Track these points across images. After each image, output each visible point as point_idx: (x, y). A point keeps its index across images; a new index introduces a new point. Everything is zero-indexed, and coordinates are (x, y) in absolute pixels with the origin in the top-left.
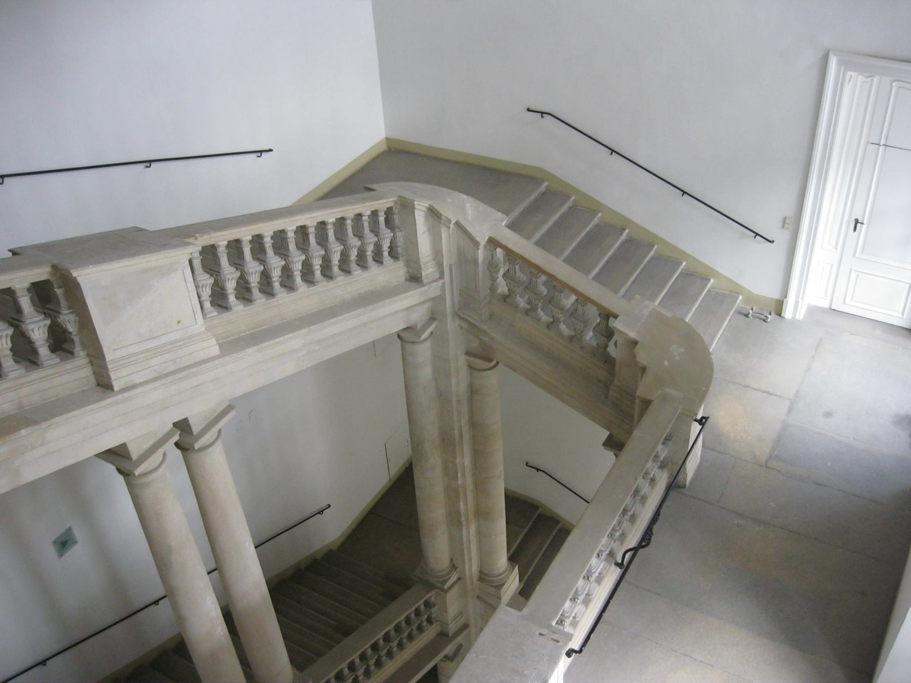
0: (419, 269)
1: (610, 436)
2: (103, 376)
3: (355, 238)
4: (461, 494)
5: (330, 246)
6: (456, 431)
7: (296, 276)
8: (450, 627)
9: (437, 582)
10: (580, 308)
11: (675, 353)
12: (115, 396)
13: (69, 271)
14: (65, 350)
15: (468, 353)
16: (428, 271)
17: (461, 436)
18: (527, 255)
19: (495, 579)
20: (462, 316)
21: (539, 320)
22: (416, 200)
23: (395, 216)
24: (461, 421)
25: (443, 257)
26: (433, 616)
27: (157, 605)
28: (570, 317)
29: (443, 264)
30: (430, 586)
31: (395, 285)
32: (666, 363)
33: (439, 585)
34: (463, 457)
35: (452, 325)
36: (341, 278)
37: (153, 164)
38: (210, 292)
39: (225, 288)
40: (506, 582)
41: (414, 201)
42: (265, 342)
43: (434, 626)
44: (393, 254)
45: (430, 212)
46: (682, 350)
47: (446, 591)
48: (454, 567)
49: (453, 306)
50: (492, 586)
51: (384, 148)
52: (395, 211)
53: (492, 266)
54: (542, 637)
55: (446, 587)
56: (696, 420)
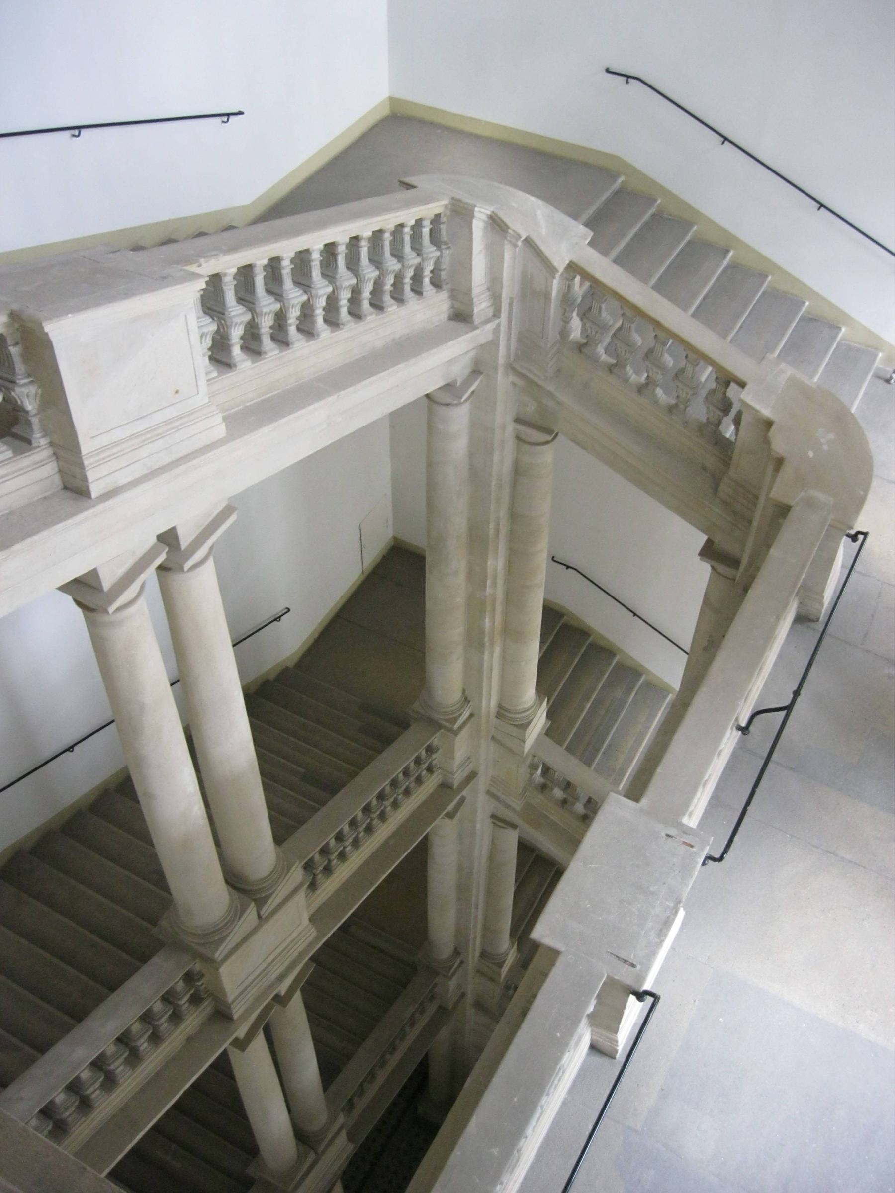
0: (470, 304)
1: (709, 543)
2: (74, 477)
3: (393, 259)
4: (488, 608)
5: (363, 271)
6: (492, 525)
7: (317, 315)
8: (455, 777)
9: (443, 720)
10: (689, 369)
11: (823, 441)
12: (94, 506)
13: (41, 324)
14: (16, 436)
15: (518, 420)
16: (481, 306)
17: (497, 532)
18: (622, 291)
19: (520, 716)
20: (520, 370)
21: (626, 381)
22: (477, 205)
23: (442, 226)
24: (499, 512)
26: (434, 762)
27: (72, 751)
28: (674, 380)
29: (500, 296)
30: (434, 725)
31: (436, 326)
32: (811, 454)
33: (447, 725)
34: (496, 559)
35: (503, 382)
36: (372, 318)
37: (83, 131)
38: (211, 343)
39: (229, 337)
40: (533, 719)
41: (475, 206)
42: (284, 416)
43: (435, 775)
44: (436, 284)
45: (491, 221)
46: (831, 436)
47: (456, 733)
48: (467, 701)
49: (508, 356)
50: (515, 725)
51: (385, 112)
52: (444, 219)
53: (566, 299)
54: (670, 839)
55: (456, 726)
56: (848, 536)
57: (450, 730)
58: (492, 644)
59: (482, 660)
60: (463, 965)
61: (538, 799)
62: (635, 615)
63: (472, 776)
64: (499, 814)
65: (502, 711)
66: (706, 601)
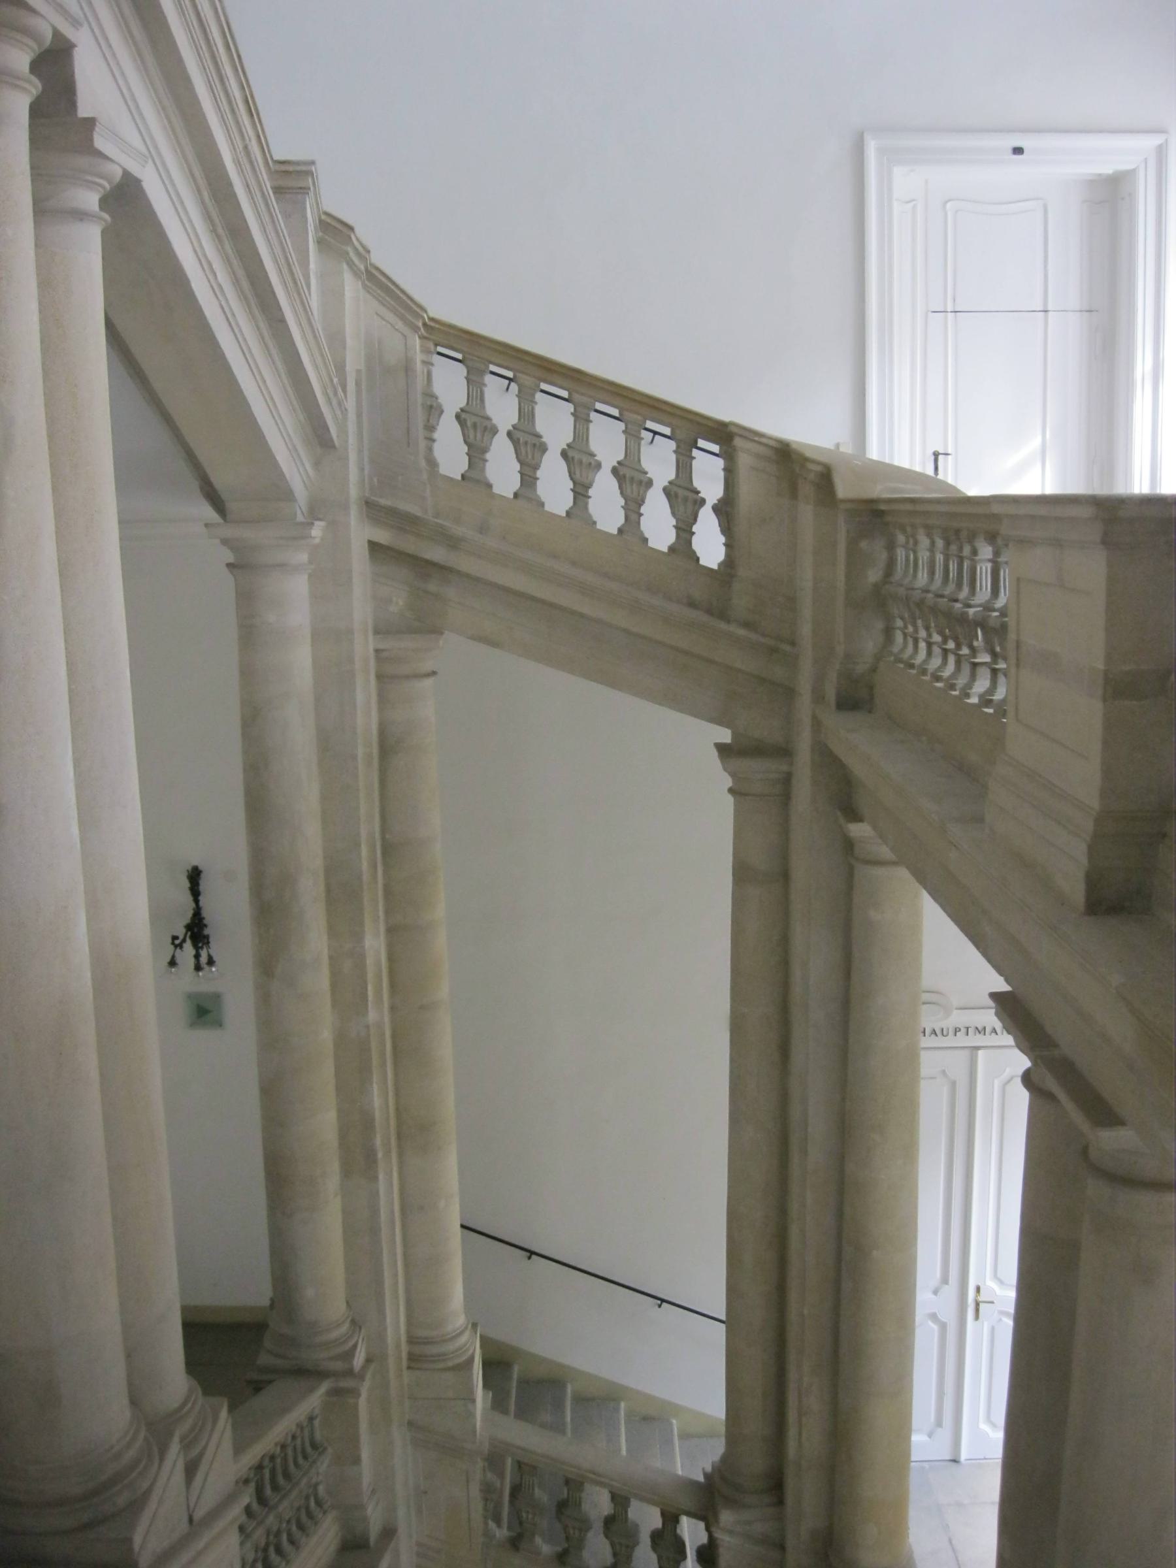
4: (375, 1061)
6: (364, 851)
9: (331, 1359)
25: (345, 348)
33: (339, 1366)
48: (356, 1324)
58: (388, 1152)
59: (375, 1195)
62: (531, 1253)
63: (389, 1533)
66: (742, 873)
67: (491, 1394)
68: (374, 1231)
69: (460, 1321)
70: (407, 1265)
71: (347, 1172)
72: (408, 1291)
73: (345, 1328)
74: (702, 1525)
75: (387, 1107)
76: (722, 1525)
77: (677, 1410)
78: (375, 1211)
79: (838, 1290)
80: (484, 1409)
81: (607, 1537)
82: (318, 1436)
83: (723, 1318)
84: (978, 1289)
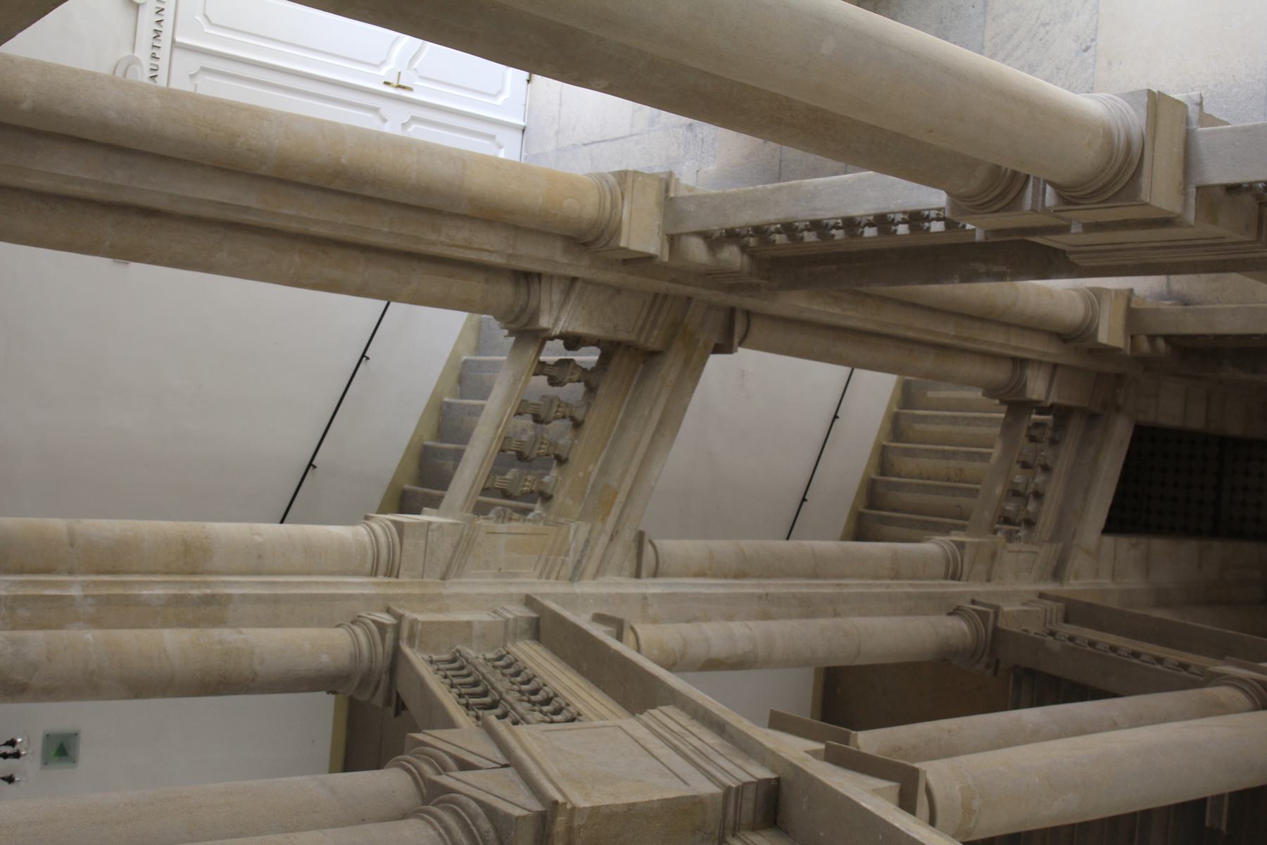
4: (118, 591)
8: (510, 616)
19: (382, 539)
33: (390, 636)
57: (397, 628)
58: (207, 584)
59: (245, 598)
60: (976, 598)
61: (560, 498)
63: (529, 601)
64: (630, 566)
65: (382, 568)
67: (425, 509)
68: (276, 599)
69: (361, 530)
70: (309, 573)
71: (220, 622)
72: (332, 573)
73: (358, 630)
74: (549, 344)
75: (166, 582)
76: (551, 326)
77: (454, 354)
78: (260, 599)
79: (372, 199)
80: (438, 515)
81: (549, 422)
82: (446, 656)
83: (384, 303)
84: (387, 83)
